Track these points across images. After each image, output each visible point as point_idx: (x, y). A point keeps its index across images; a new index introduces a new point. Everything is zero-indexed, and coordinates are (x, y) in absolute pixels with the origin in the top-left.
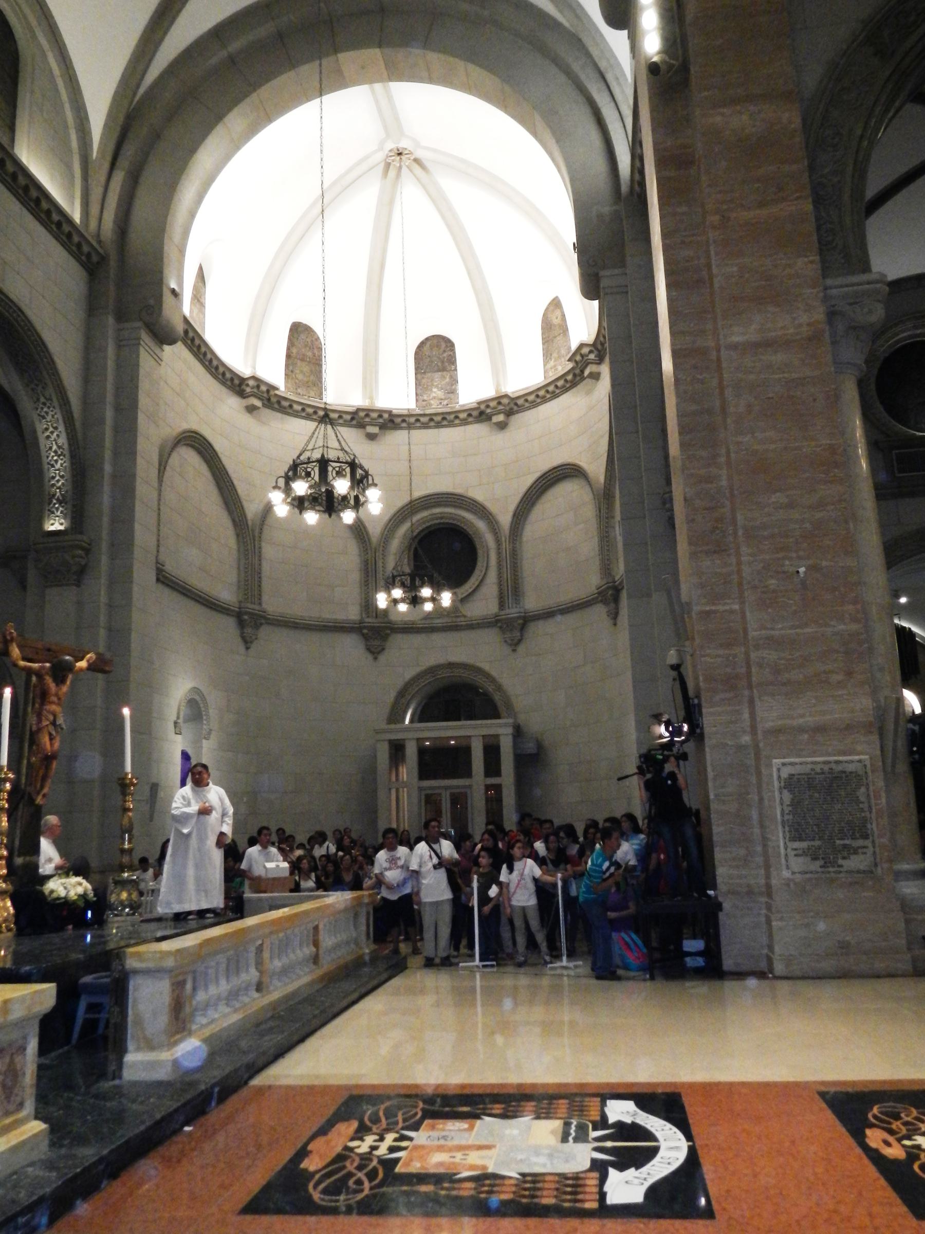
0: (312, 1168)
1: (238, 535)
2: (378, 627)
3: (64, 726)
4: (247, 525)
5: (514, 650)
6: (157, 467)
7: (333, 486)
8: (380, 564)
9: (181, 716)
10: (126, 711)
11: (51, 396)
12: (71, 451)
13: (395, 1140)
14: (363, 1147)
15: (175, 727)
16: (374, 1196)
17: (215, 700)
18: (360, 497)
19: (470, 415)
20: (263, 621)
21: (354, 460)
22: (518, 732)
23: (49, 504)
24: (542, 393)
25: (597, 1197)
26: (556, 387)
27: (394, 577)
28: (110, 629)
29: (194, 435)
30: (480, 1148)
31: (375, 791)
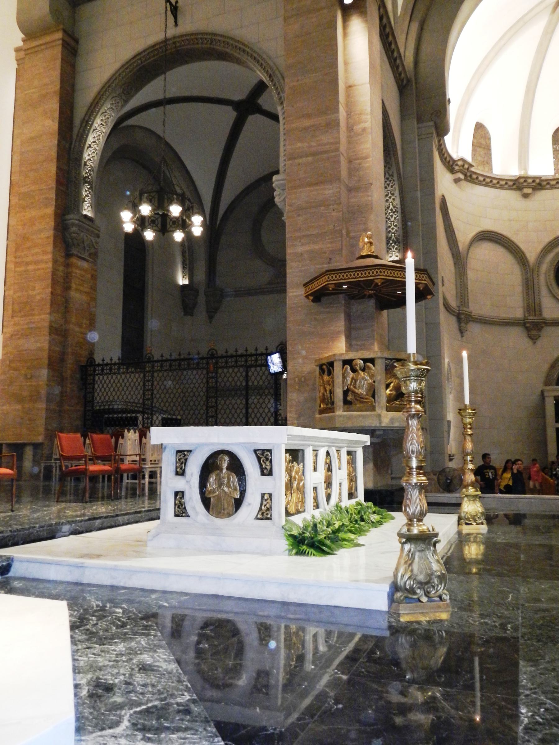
1: (455, 264)
2: (537, 322)
8: (536, 281)
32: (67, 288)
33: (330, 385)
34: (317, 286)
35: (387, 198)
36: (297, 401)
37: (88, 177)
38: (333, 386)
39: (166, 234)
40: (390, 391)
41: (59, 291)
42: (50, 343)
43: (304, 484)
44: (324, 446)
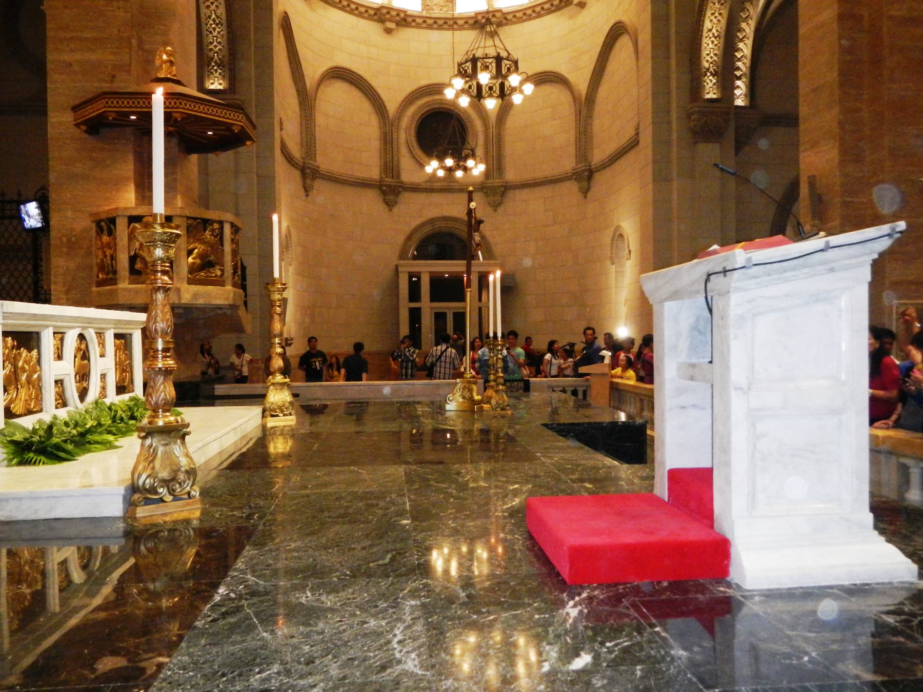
1: (300, 104)
5: (495, 210)
8: (395, 136)
12: (227, 21)
19: (466, 22)
23: (209, 66)
24: (529, 12)
26: (543, 8)
33: (111, 248)
34: (93, 111)
36: (65, 268)
38: (115, 249)
40: (194, 258)
43: (40, 378)
44: (74, 328)
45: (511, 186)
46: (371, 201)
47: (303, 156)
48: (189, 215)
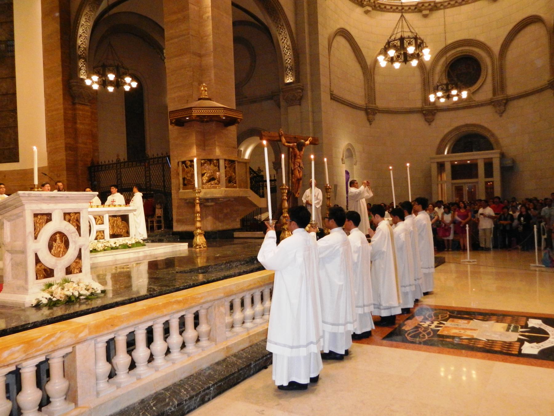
0: (406, 329)
1: (364, 73)
3: (303, 167)
4: (368, 67)
5: (501, 116)
6: (327, 48)
7: (407, 51)
8: (431, 79)
9: (344, 156)
10: (325, 160)
11: (283, 24)
12: (292, 47)
13: (438, 324)
14: (426, 325)
15: (342, 161)
16: (430, 340)
17: (358, 148)
18: (420, 53)
20: (377, 112)
21: (416, 36)
22: (503, 156)
23: (286, 71)
25: (518, 350)
27: (438, 86)
28: (314, 122)
29: (343, 30)
30: (471, 329)
31: (430, 186)
32: (76, 123)
35: (283, 41)
37: (82, 55)
39: (119, 87)
41: (70, 125)
42: (66, 156)
45: (510, 99)
46: (417, 121)
47: (366, 102)
48: (201, 159)
